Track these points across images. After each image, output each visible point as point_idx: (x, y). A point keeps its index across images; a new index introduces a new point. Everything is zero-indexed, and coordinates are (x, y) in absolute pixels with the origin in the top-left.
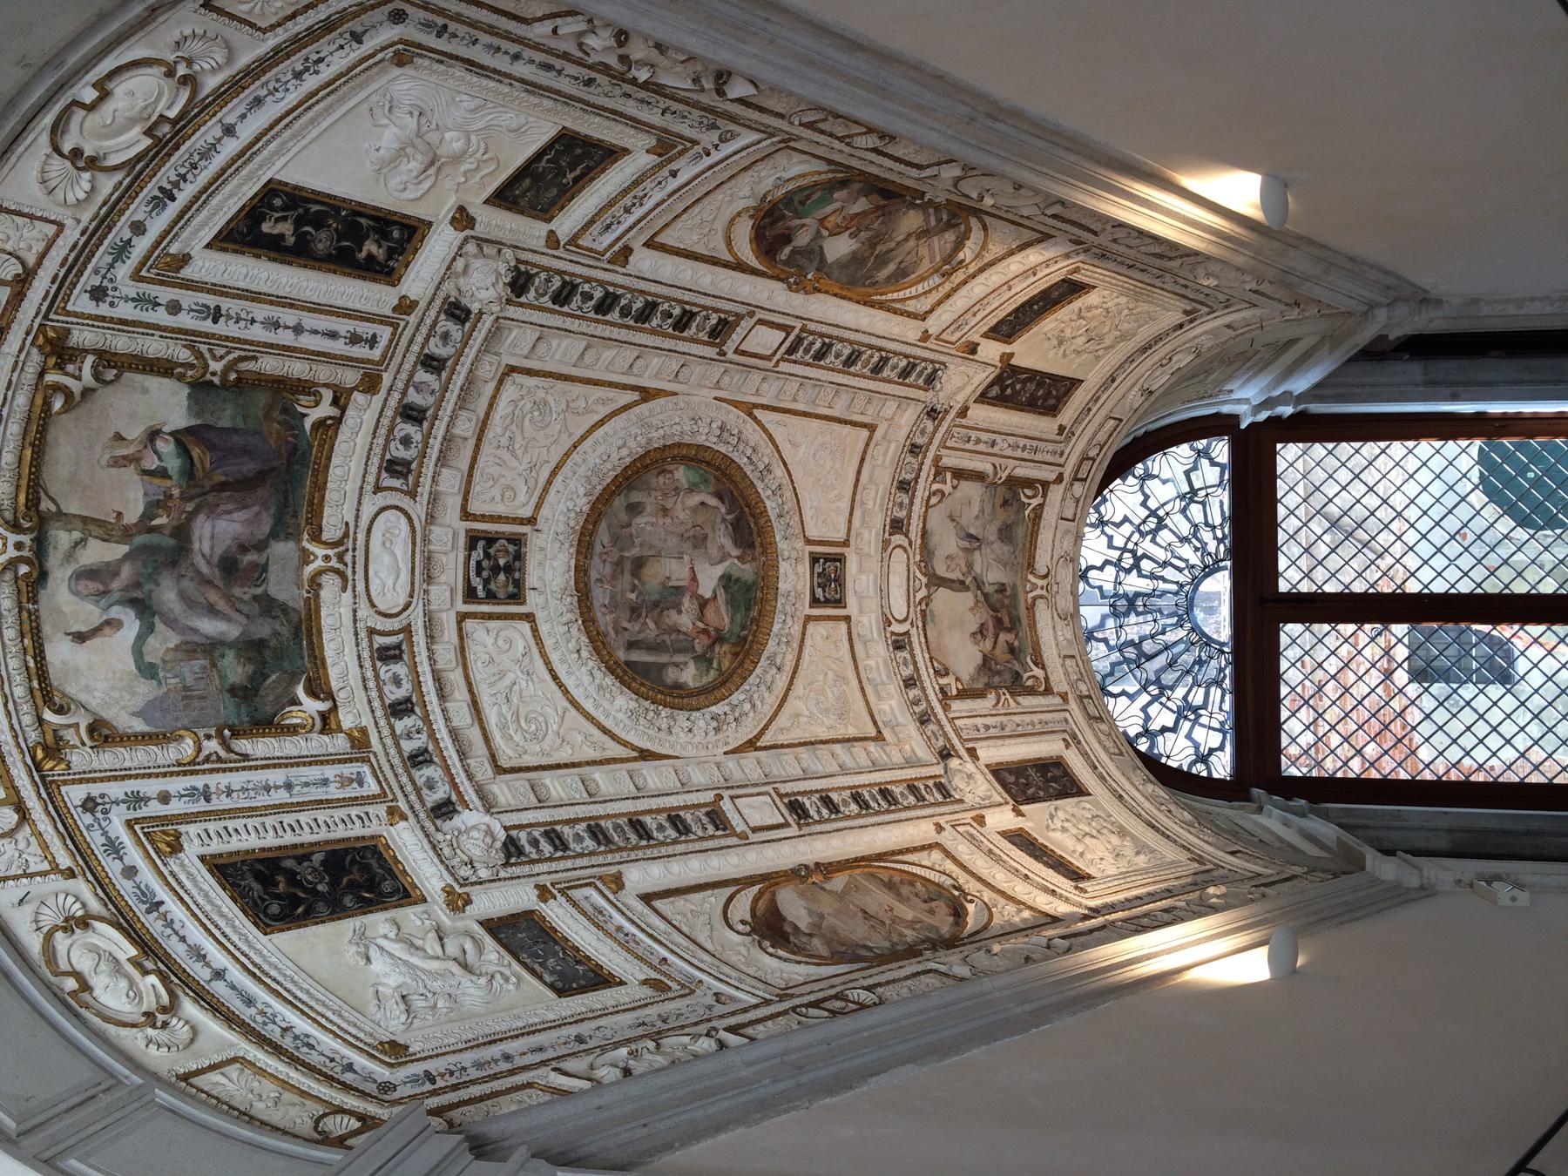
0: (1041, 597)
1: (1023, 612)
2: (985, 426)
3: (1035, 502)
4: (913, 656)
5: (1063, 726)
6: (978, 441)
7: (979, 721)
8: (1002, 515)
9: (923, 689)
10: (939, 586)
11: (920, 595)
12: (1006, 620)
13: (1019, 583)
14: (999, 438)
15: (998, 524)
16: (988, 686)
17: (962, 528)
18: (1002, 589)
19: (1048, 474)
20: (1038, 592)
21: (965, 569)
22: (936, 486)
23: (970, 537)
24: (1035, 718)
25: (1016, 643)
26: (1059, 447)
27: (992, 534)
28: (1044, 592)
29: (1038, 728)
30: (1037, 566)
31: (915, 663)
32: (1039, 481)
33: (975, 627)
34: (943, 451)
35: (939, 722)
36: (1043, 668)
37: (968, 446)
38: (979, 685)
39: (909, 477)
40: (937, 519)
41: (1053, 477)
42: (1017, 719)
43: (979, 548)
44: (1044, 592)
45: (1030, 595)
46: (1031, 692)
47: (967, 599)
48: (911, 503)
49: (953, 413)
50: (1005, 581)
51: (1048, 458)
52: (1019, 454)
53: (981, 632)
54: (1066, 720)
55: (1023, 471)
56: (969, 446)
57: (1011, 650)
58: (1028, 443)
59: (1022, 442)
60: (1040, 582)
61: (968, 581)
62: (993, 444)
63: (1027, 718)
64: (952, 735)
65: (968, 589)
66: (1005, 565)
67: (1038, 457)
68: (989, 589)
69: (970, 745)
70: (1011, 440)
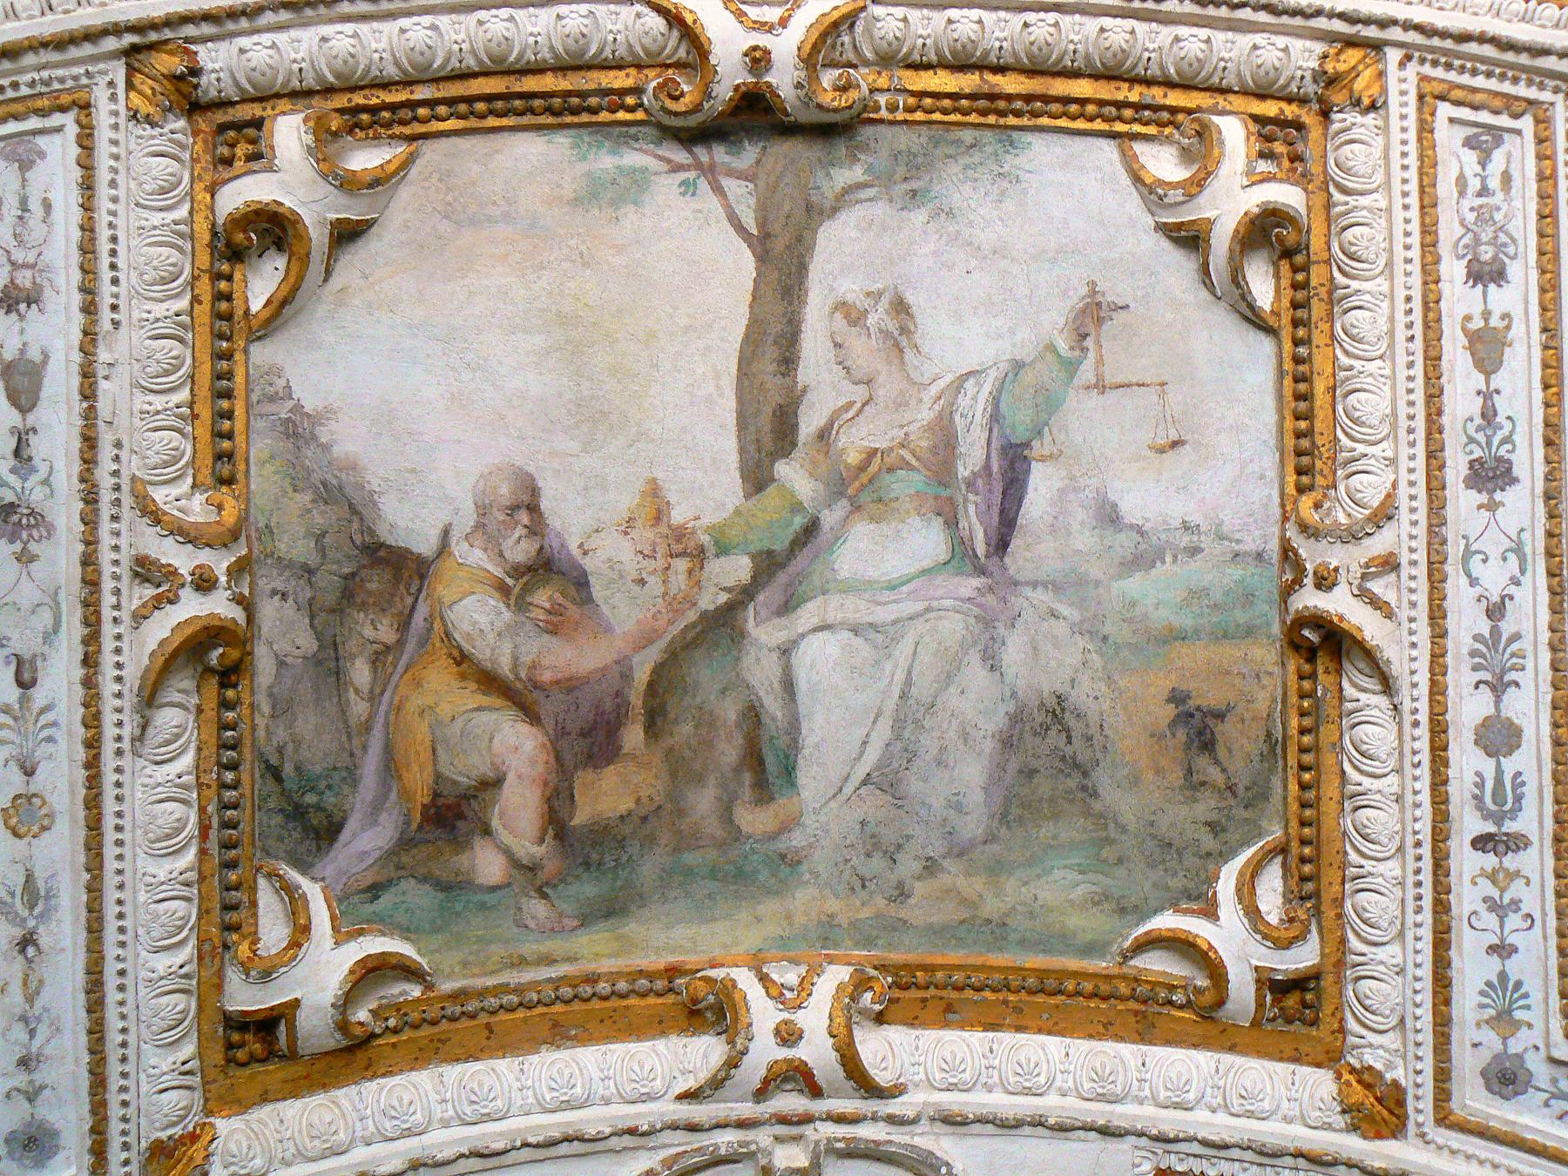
1: (661, 939)
3: (1227, 935)
8: (1125, 711)
10: (761, 244)
12: (606, 795)
13: (806, 902)
15: (1088, 695)
17: (1047, 404)
18: (766, 763)
20: (763, 1014)
21: (853, 443)
23: (1012, 468)
25: (488, 865)
27: (1047, 654)
28: (764, 1052)
30: (896, 1035)
32: (1338, 957)
37: (1453, 270)
38: (260, 447)
41: (1375, 1051)
43: (961, 556)
45: (745, 980)
46: (224, 923)
47: (708, 489)
51: (1472, 970)
52: (1469, 707)
53: (547, 577)
55: (1374, 729)
57: (452, 814)
60: (815, 1018)
61: (794, 475)
65: (757, 479)
66: (886, 781)
67: (1466, 862)
68: (764, 632)
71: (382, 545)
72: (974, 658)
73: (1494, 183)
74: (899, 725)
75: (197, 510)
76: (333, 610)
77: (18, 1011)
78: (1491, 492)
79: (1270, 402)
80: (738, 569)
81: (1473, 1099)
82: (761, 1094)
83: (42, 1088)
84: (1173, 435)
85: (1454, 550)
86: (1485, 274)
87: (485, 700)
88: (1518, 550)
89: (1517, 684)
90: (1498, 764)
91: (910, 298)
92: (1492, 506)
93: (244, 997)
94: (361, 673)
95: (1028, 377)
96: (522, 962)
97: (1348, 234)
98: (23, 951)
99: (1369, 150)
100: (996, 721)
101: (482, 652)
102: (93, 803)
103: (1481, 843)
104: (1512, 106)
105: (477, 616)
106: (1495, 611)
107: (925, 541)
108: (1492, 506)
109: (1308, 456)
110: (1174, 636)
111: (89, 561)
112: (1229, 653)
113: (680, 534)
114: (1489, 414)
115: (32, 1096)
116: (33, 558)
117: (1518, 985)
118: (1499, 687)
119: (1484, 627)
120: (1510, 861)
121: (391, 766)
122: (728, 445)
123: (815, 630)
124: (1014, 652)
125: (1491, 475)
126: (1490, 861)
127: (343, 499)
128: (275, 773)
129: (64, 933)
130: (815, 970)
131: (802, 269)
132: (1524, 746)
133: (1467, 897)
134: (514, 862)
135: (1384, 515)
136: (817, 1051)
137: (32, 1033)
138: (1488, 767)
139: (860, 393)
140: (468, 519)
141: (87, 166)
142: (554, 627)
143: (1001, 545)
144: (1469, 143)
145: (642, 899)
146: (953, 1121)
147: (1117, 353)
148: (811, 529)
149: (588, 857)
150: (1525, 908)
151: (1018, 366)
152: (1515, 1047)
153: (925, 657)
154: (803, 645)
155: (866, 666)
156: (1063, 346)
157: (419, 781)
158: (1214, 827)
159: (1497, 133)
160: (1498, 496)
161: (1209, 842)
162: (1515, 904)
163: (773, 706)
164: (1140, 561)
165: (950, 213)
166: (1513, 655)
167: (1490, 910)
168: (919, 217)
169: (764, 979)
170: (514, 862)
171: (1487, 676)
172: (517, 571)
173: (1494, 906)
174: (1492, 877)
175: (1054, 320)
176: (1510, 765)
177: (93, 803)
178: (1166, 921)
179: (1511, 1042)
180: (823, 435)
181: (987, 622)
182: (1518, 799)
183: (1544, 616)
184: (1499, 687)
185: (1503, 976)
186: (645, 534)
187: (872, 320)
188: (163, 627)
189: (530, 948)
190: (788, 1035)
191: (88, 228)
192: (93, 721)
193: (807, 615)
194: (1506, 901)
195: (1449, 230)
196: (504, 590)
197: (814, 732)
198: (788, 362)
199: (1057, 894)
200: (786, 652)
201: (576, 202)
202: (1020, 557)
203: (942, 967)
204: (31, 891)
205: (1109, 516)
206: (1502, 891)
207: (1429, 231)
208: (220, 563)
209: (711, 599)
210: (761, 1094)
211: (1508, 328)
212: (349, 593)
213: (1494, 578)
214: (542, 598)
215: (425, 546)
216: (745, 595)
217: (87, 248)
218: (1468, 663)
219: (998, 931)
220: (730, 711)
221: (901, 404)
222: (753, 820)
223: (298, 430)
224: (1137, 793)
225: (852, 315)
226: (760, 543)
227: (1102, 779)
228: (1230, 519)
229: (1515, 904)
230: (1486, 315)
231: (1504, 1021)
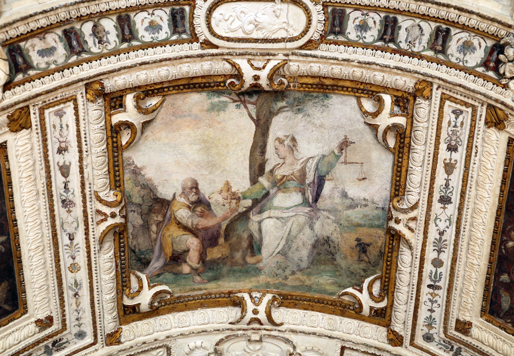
0: (244, 311)
1: (227, 285)
2: (473, 172)
3: (364, 297)
4: (162, 44)
5: (72, 329)
6: (449, 168)
7: (72, 157)
8: (345, 241)
9: (116, 53)
10: (257, 122)
11: (243, 63)
12: (214, 253)
13: (262, 279)
14: (452, 209)
16: (125, 203)
17: (331, 166)
18: (254, 247)
19: (401, 322)
20: (250, 306)
21: (279, 173)
22: (387, 99)
24: (82, 275)
25: (186, 269)
26: (437, 332)
27: (325, 227)
28: (250, 315)
29: (68, 278)
30: (282, 310)
31: (153, 45)
32: (391, 305)
33: (206, 190)
34: (437, 95)
35: (69, 67)
36: (154, 311)
37: (443, 146)
39: (402, 35)
40: (343, 110)
41: (398, 327)
42: (80, 238)
43: (305, 202)
44: (250, 315)
45: (246, 296)
46: (122, 285)
47: (241, 183)
48: (366, 46)
49: (495, 92)
50: (265, 252)
51: (423, 314)
52: (431, 255)
53: (200, 204)
54: (81, 335)
55: (406, 259)
56: (444, 154)
57: (177, 258)
58: (445, 270)
59: (446, 257)
60: (262, 308)
61: (264, 181)
62: (445, 200)
63: (81, 259)
64: (48, 83)
65: (254, 181)
66: (283, 253)
67: (425, 290)
68: (254, 218)
69: (34, 119)
70: (450, 235)
71: (158, 198)
72: (307, 227)
73: (458, 124)
74: (287, 241)
75: (111, 198)
76: (146, 215)
77: (75, 309)
78: (445, 204)
79: (390, 170)
80: (248, 203)
81: (419, 341)
82: (249, 324)
83: (82, 324)
84: (364, 176)
85: (433, 218)
86: (452, 149)
87: (185, 233)
88: (450, 220)
89: (444, 252)
90: (437, 269)
91: (296, 137)
92: (444, 208)
93: (127, 302)
94: (154, 228)
95: (326, 159)
96: (194, 290)
97: (416, 132)
98: (75, 297)
99: (425, 110)
100: (312, 241)
101: (184, 222)
102: (89, 265)
103: (429, 286)
104: (466, 104)
105: (183, 214)
106: (441, 234)
107: (296, 198)
108: (444, 208)
109: (399, 187)
110: (359, 225)
111: (85, 212)
112: (373, 231)
113: (234, 194)
114: (447, 185)
115: (79, 326)
116: (71, 211)
117: (434, 319)
118: (439, 251)
119: (438, 237)
120: (436, 292)
121: (162, 248)
122: (247, 173)
123: (267, 218)
124: (317, 226)
125: (445, 200)
126: (431, 291)
127: (148, 188)
128: (134, 251)
129: (85, 292)
130: (264, 295)
131: (268, 129)
132: (444, 266)
133: (424, 297)
134: (192, 268)
135: (414, 207)
136: (262, 316)
137: (79, 313)
138: (434, 270)
139: (281, 161)
140: (180, 191)
141: (77, 114)
142: (202, 215)
143: (316, 200)
144: (454, 112)
145: (223, 276)
146: (293, 331)
147: (350, 154)
148: (267, 194)
149: (209, 268)
150: (438, 303)
151: (324, 156)
152: (431, 332)
153: (295, 226)
154: (264, 221)
155: (279, 226)
156: (336, 152)
157: (169, 251)
158: (365, 270)
159: (461, 112)
160: (446, 206)
161: (363, 273)
162: (436, 301)
163: (256, 235)
164: (351, 207)
165: (309, 115)
166: (444, 245)
167: (430, 301)
168: (300, 116)
169: (251, 297)
170: (192, 268)
171: (437, 248)
172: (192, 203)
173: (431, 301)
174: (431, 294)
175: (334, 145)
176: (439, 270)
177: (89, 265)
178: (350, 290)
179: (430, 331)
180: (272, 171)
181: (311, 218)
182: (440, 278)
183: (453, 237)
184: (439, 251)
185: (431, 316)
186: (225, 194)
187: (286, 143)
188: (103, 226)
189: (196, 287)
190: (255, 312)
191: (78, 131)
192: (88, 247)
193: (265, 214)
194: (434, 300)
195: (444, 135)
196: (189, 208)
197: (266, 242)
198: (263, 152)
199: (324, 281)
200: (260, 223)
201: (208, 110)
202: (321, 204)
203: (294, 295)
204: (76, 284)
205: (345, 195)
206: (433, 298)
207: (438, 136)
208: (117, 210)
209: (241, 210)
210: (249, 324)
211: (456, 164)
212: (151, 210)
213: (442, 226)
214: (199, 209)
215: (169, 198)
216: (249, 209)
217: (79, 136)
218: (433, 244)
219: (309, 288)
220: (245, 236)
221: (292, 164)
222: (250, 260)
223: (136, 172)
224: (347, 260)
225: (281, 141)
226: (254, 196)
227: (338, 257)
228: (376, 199)
229: (436, 301)
230: (451, 159)
231: (430, 326)
